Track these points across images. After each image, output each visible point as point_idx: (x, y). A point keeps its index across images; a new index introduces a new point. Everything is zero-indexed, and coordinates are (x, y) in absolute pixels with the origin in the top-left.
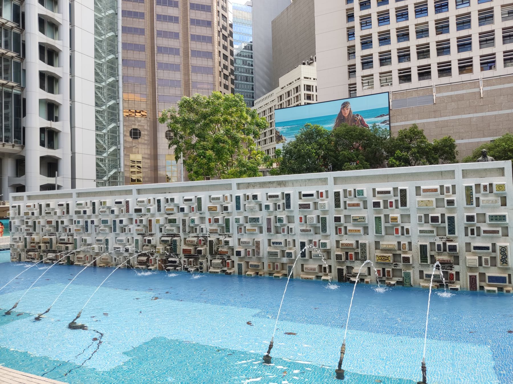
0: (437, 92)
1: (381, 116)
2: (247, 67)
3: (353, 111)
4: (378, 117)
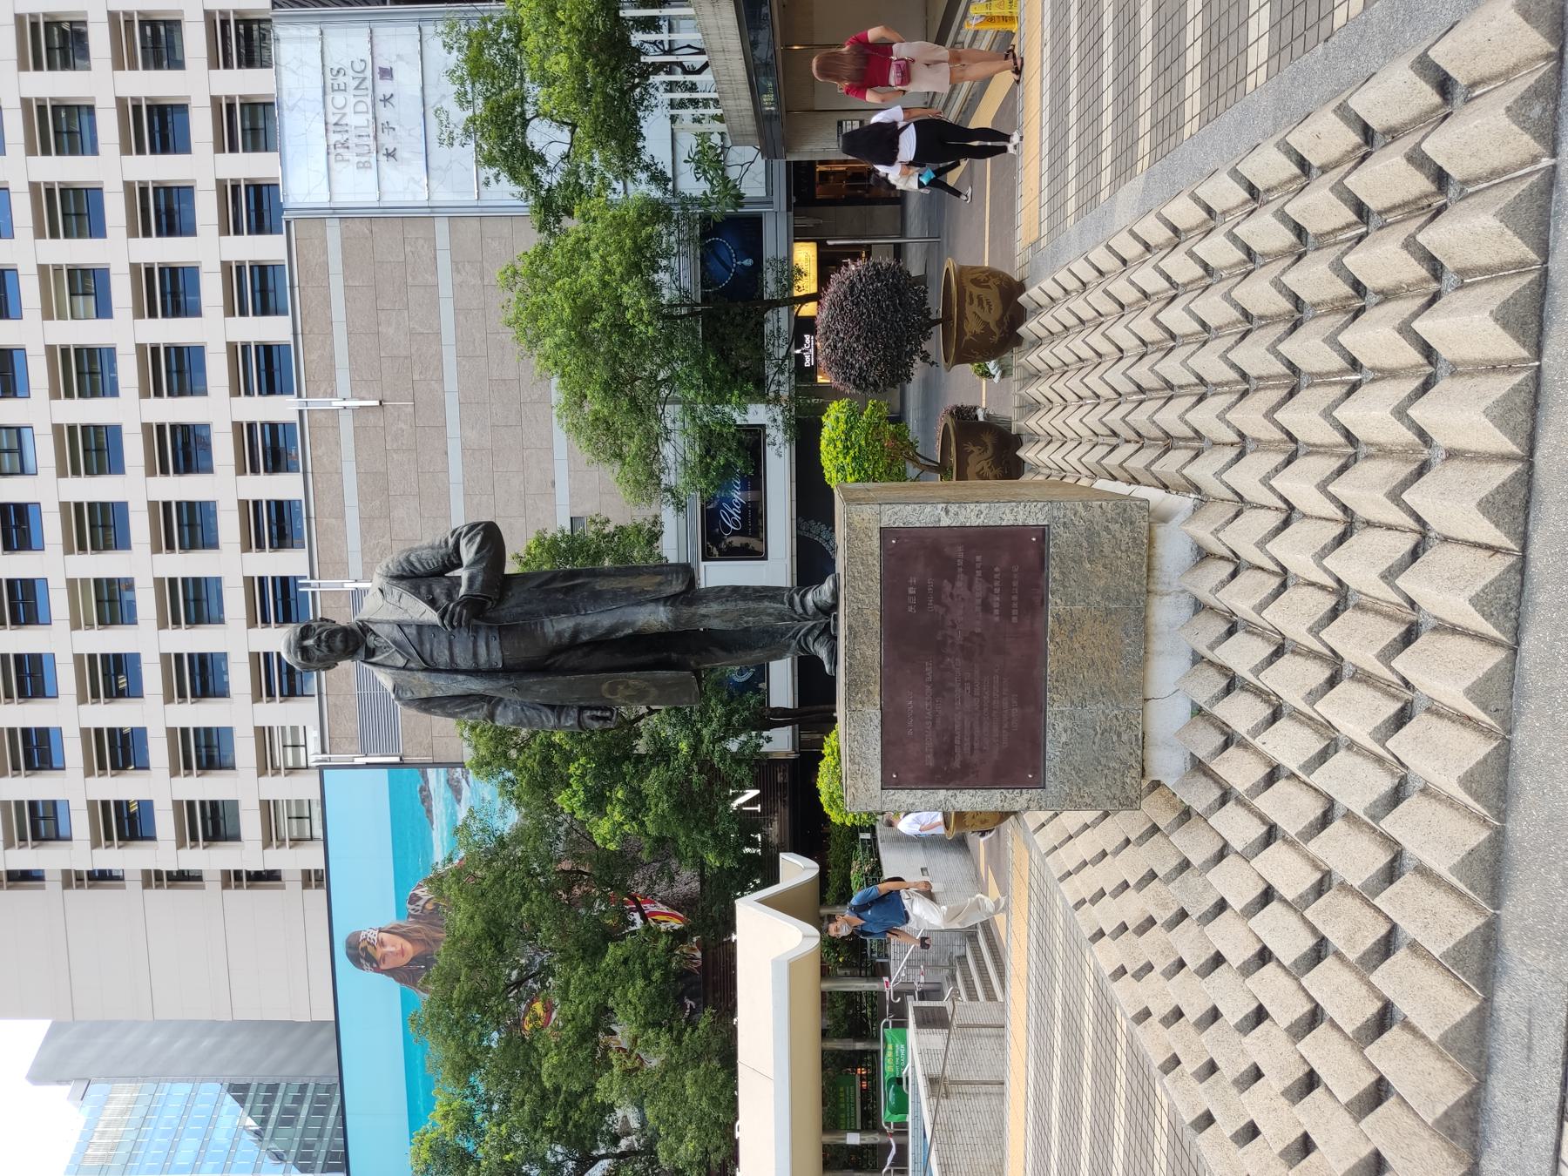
0: (342, 570)
1: (426, 798)
2: (306, 1106)
3: (390, 918)
4: (429, 811)
